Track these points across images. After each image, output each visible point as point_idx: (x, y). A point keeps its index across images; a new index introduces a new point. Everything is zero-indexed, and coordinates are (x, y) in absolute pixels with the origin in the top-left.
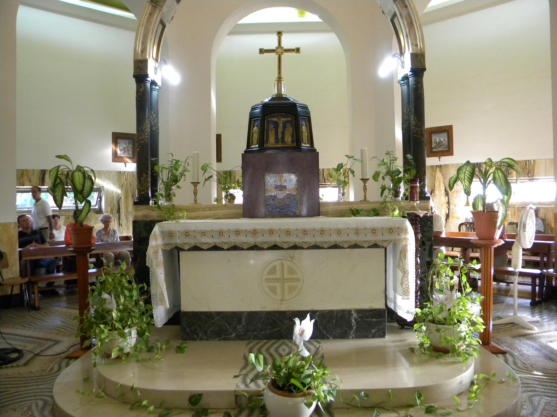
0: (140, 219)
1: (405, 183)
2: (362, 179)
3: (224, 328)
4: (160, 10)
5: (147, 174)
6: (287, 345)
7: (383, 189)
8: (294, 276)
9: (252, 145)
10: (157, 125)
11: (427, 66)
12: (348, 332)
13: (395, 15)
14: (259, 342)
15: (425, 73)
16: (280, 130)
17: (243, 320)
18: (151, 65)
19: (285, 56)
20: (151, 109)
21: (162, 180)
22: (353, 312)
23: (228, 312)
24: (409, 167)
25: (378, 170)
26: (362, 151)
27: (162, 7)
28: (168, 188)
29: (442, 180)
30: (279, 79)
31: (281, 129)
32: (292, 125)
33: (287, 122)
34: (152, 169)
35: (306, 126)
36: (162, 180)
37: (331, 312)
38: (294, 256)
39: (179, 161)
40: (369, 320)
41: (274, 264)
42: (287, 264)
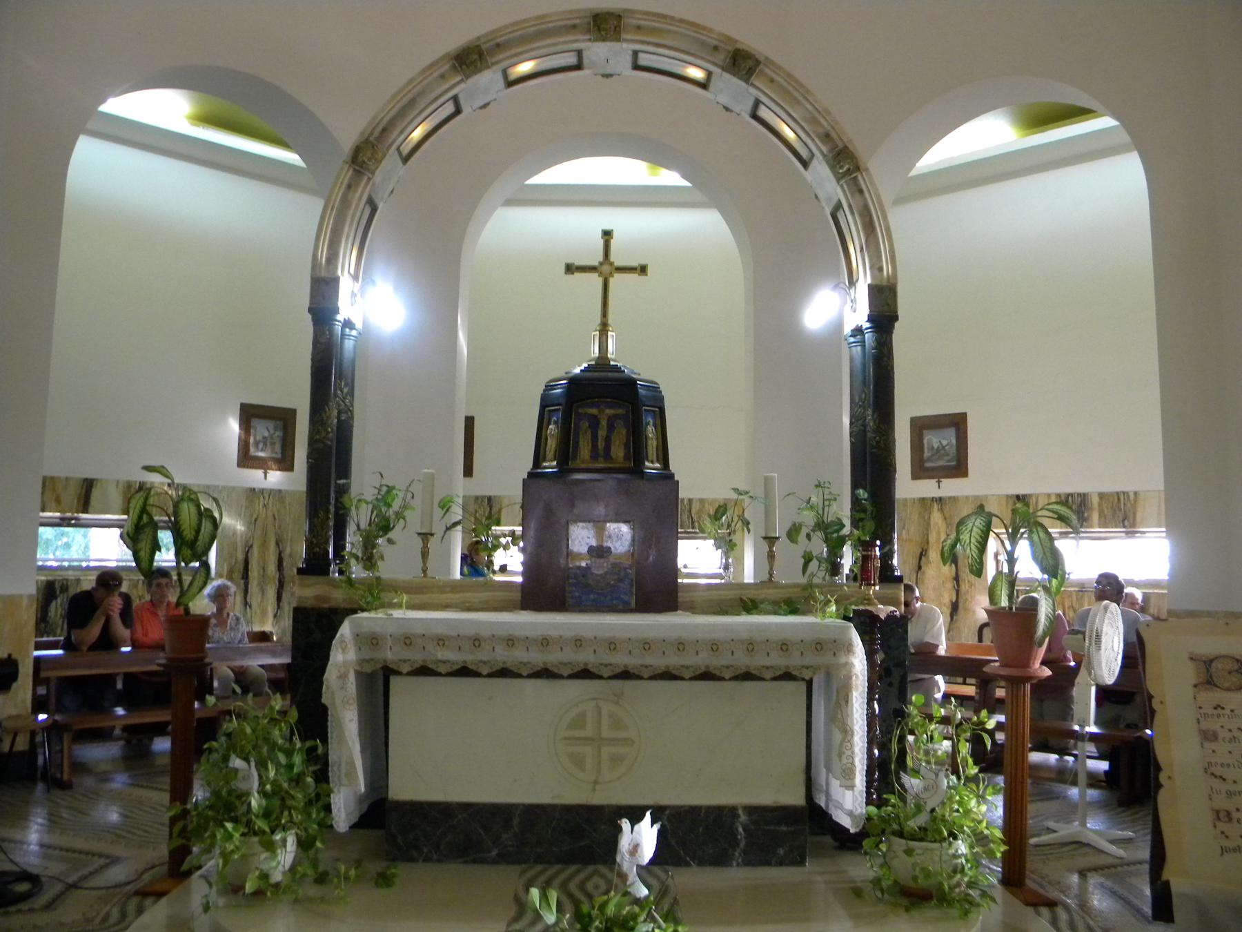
0: (309, 604)
1: (854, 547)
2: (765, 538)
4: (369, 179)
5: (327, 511)
6: (603, 876)
7: (808, 559)
8: (624, 735)
9: (544, 460)
10: (349, 411)
11: (900, 313)
13: (839, 206)
14: (546, 870)
15: (897, 325)
16: (602, 433)
17: (516, 821)
18: (346, 286)
19: (616, 281)
20: (340, 376)
21: (358, 526)
22: (740, 812)
24: (862, 515)
25: (798, 520)
26: (767, 481)
27: (373, 173)
28: (369, 544)
30: (604, 328)
31: (603, 425)
33: (616, 416)
34: (337, 500)
35: (655, 425)
36: (358, 526)
37: (694, 810)
39: (393, 488)
40: (772, 828)
42: (606, 708)
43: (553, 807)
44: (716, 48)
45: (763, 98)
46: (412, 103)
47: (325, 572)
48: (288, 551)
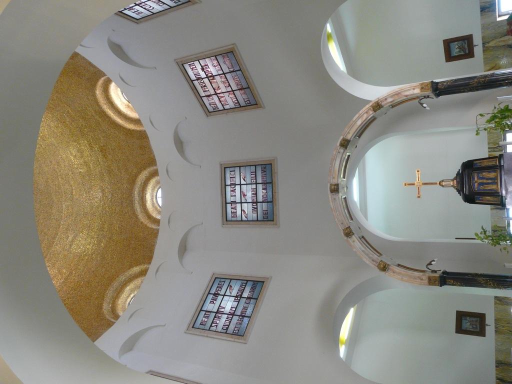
16: (485, 181)
29: (498, 40)
32: (482, 173)
46: (363, 251)
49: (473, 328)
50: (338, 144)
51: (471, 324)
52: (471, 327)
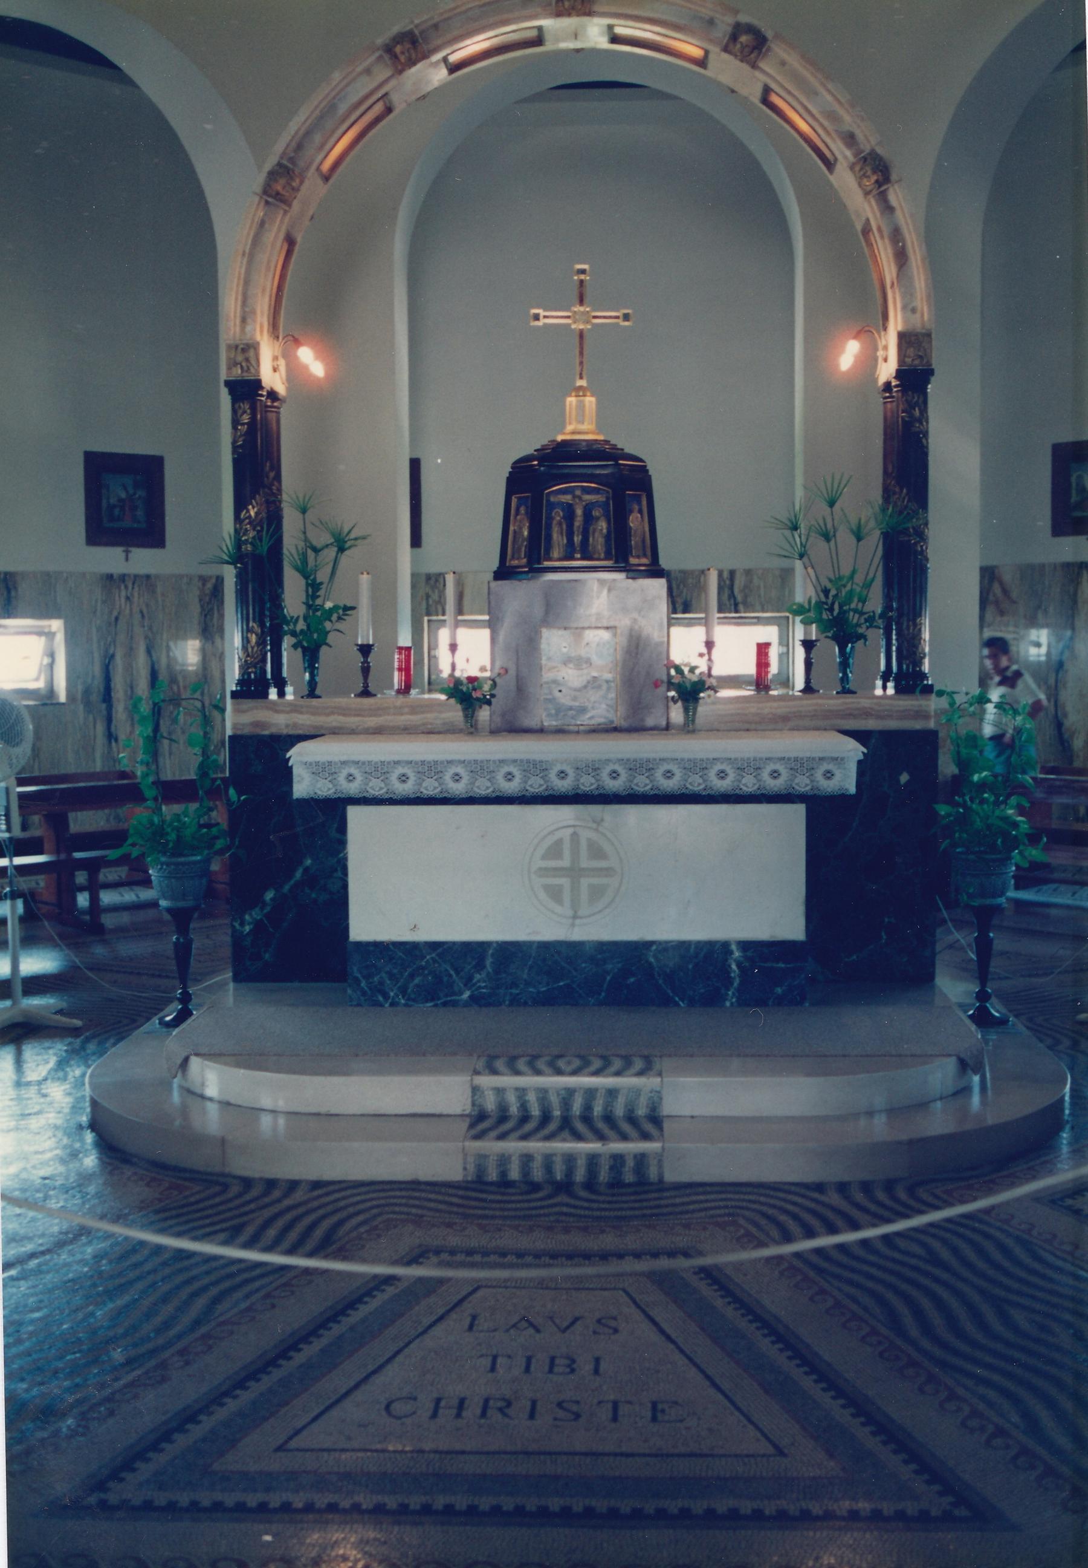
0: (246, 731)
3: (445, 979)
4: (286, 212)
8: (603, 864)
12: (723, 991)
17: (489, 961)
22: (734, 947)
23: (454, 943)
38: (602, 820)
40: (769, 964)
41: (558, 835)
42: (585, 835)
43: (529, 944)
44: (711, 22)
45: (773, 86)
47: (265, 695)
48: (164, 661)
49: (111, 508)
50: (744, 18)
51: (120, 500)
52: (113, 501)
